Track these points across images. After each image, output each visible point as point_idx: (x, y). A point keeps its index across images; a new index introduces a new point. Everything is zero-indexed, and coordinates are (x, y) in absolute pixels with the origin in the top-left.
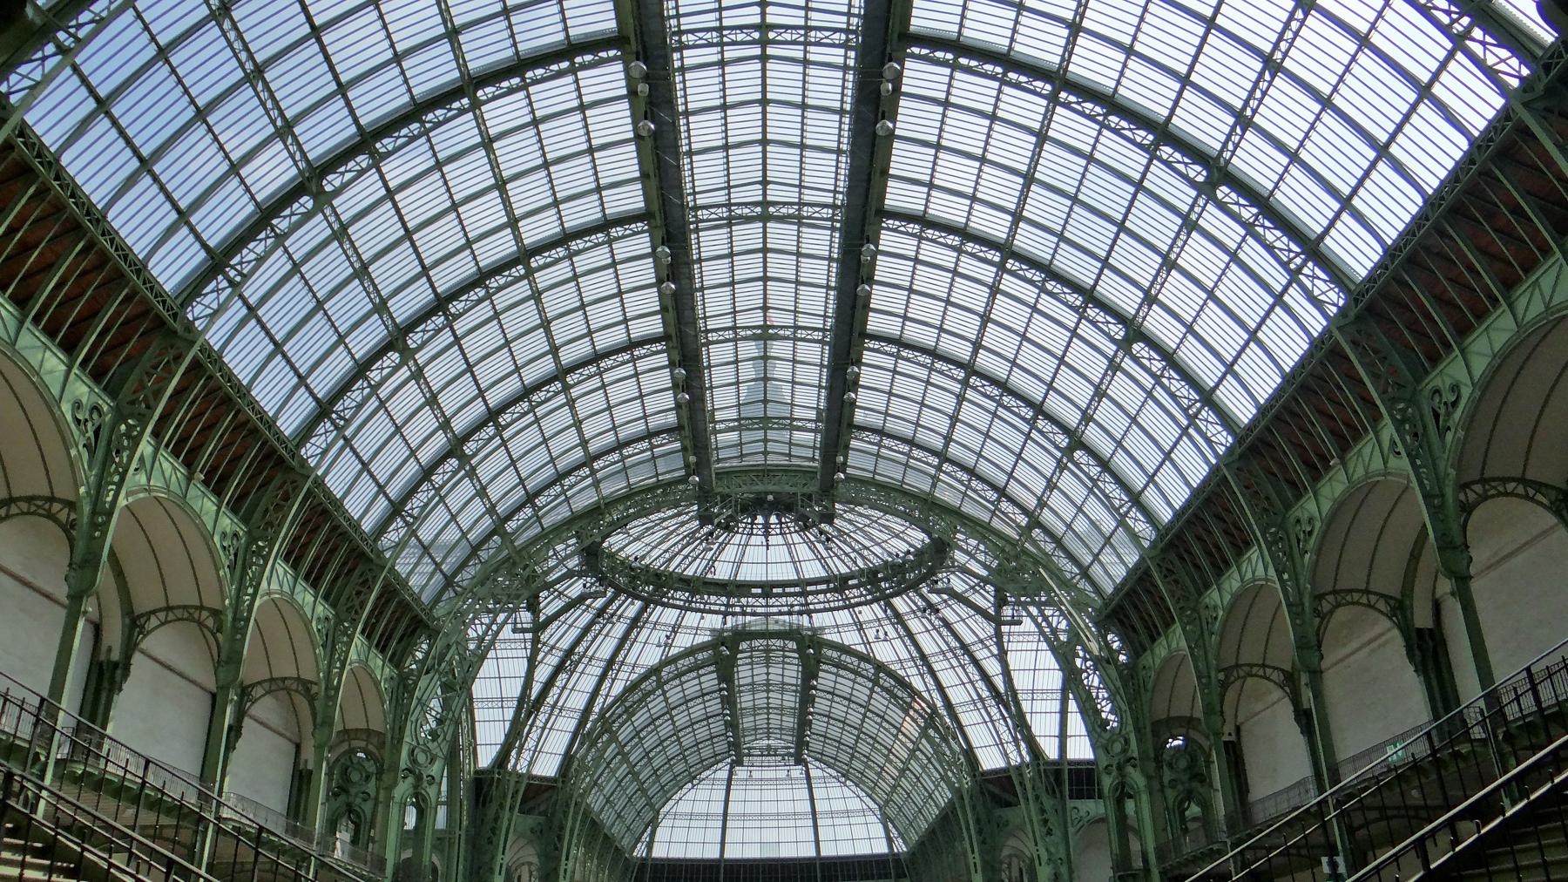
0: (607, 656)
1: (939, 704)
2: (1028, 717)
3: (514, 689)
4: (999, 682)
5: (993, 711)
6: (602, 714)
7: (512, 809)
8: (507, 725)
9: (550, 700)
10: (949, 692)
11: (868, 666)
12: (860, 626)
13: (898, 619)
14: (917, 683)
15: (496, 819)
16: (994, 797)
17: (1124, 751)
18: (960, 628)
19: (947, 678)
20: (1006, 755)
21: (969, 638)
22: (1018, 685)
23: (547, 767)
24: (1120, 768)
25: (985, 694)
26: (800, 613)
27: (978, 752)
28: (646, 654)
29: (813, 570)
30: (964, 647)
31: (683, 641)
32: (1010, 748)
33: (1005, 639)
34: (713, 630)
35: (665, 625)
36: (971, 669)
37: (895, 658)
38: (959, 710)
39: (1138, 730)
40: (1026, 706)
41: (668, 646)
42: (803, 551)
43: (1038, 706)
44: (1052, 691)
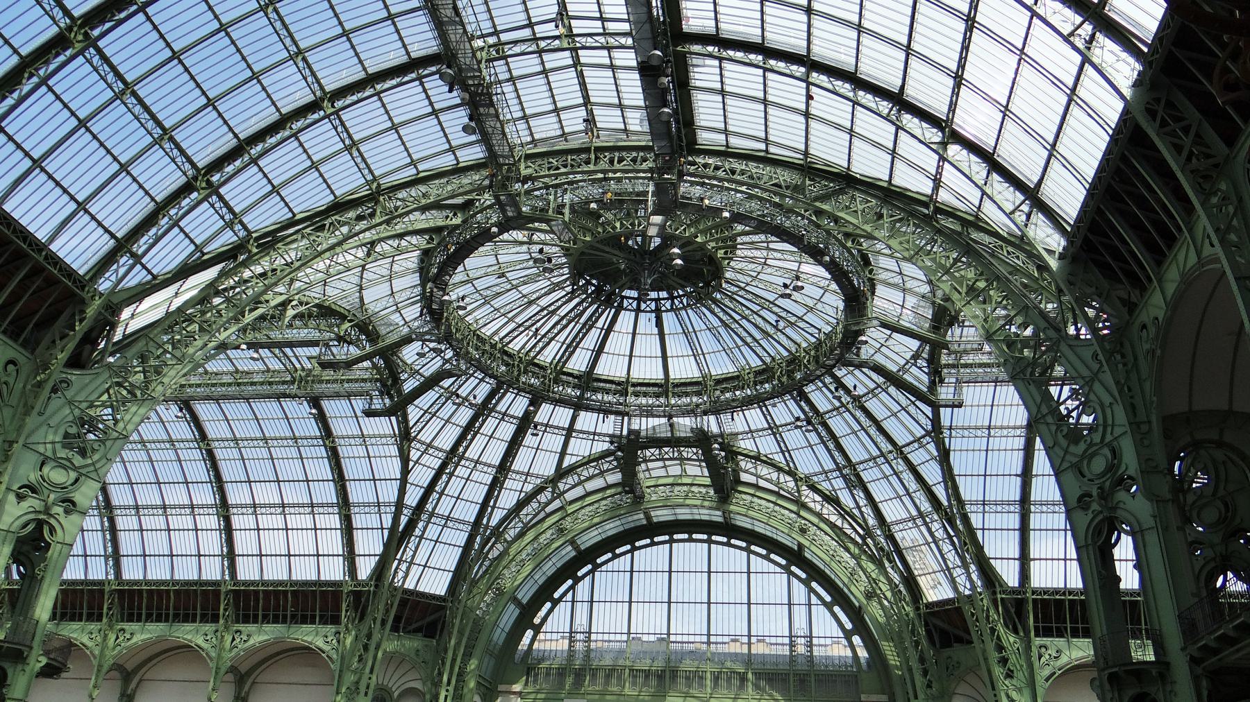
0: (496, 461)
1: (871, 521)
2: (979, 534)
3: (389, 493)
5: (935, 526)
6: (497, 532)
7: (383, 622)
8: (386, 533)
9: (429, 507)
10: (884, 508)
11: (788, 478)
12: (774, 429)
13: (815, 420)
14: (845, 498)
15: (369, 636)
16: (944, 634)
17: (1111, 468)
18: (890, 426)
19: (880, 491)
20: (953, 582)
21: (901, 438)
22: (966, 494)
23: (436, 584)
24: (1105, 496)
25: (926, 506)
26: (705, 413)
27: (923, 582)
28: (537, 458)
29: (721, 366)
30: (899, 450)
31: (580, 448)
32: (958, 572)
33: (946, 433)
34: (613, 438)
35: (558, 428)
36: (908, 477)
37: (818, 469)
38: (895, 528)
39: (1135, 425)
40: (976, 520)
41: (563, 453)
42: (707, 342)
43: (992, 520)
44: (1009, 503)
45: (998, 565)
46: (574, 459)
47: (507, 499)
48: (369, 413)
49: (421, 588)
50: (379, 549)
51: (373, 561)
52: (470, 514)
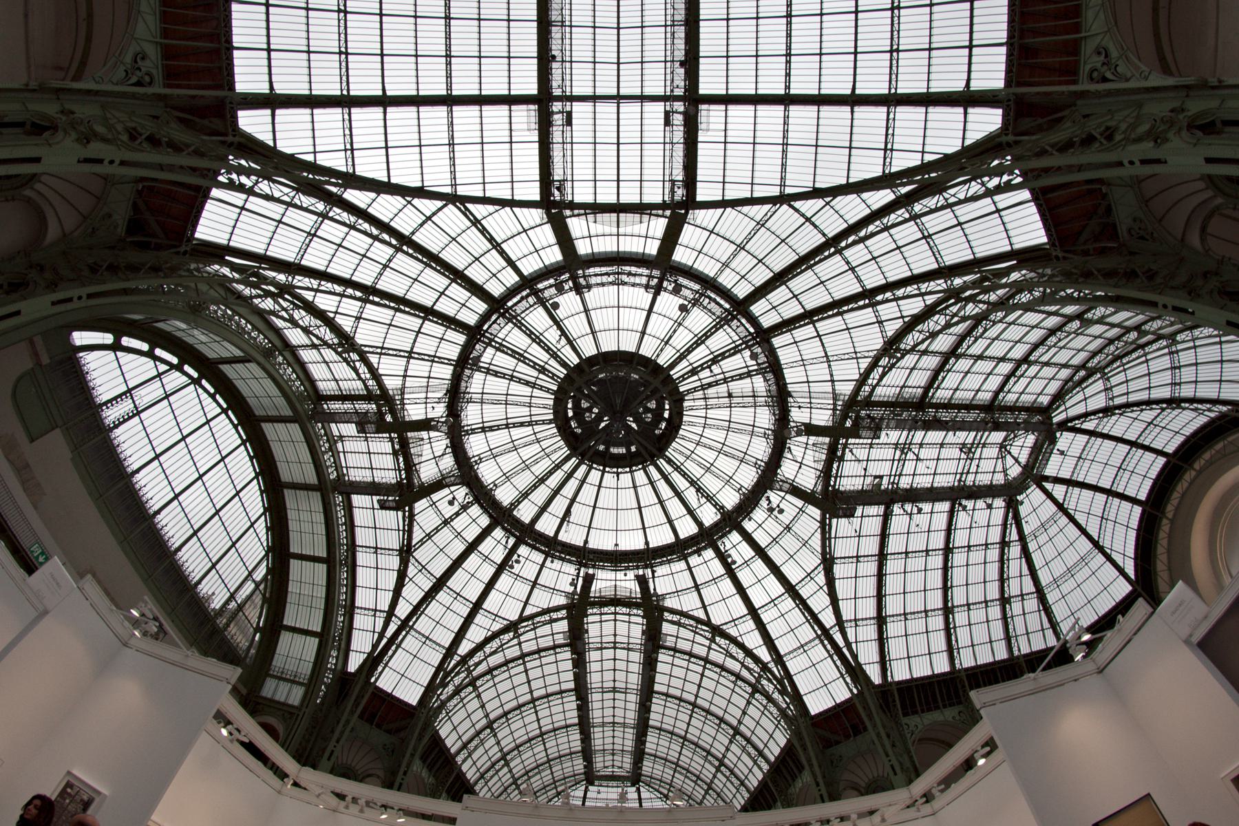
2: (854, 646)
3: (384, 602)
4: (828, 619)
8: (376, 635)
14: (753, 640)
23: (411, 694)
31: (541, 600)
40: (851, 633)
41: (526, 603)
45: (867, 668)
46: (535, 610)
47: (475, 634)
48: (383, 506)
49: (397, 694)
50: (368, 649)
51: (363, 657)
52: (447, 639)
